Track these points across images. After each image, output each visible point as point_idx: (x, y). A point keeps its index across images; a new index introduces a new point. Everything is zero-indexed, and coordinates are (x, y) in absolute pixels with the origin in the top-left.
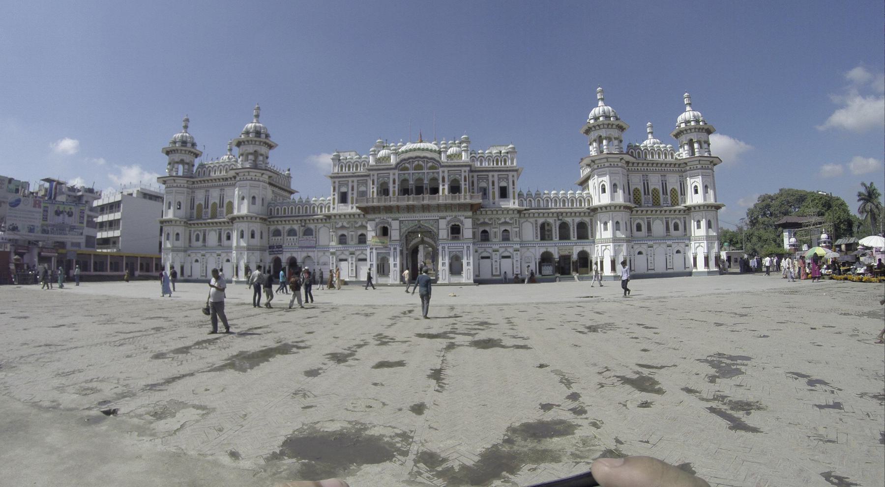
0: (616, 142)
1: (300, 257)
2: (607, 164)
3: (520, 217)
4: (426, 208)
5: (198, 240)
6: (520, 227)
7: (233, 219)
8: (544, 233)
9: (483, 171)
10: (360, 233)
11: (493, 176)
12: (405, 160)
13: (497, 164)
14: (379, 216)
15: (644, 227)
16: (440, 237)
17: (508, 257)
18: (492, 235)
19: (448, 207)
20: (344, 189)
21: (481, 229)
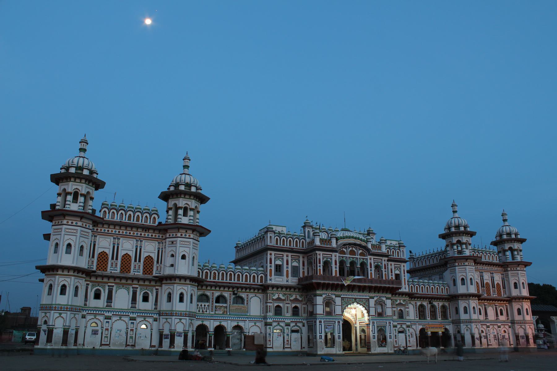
1: (229, 326)
2: (467, 264)
5: (97, 296)
7: (161, 280)
10: (294, 305)
12: (345, 245)
20: (279, 262)
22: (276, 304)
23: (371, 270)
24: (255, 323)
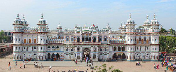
0: (133, 29)
1: (55, 53)
5: (25, 48)
6: (109, 47)
7: (37, 44)
8: (115, 49)
15: (139, 48)
17: (106, 55)
19: (93, 44)
20: (67, 38)
21: (100, 48)
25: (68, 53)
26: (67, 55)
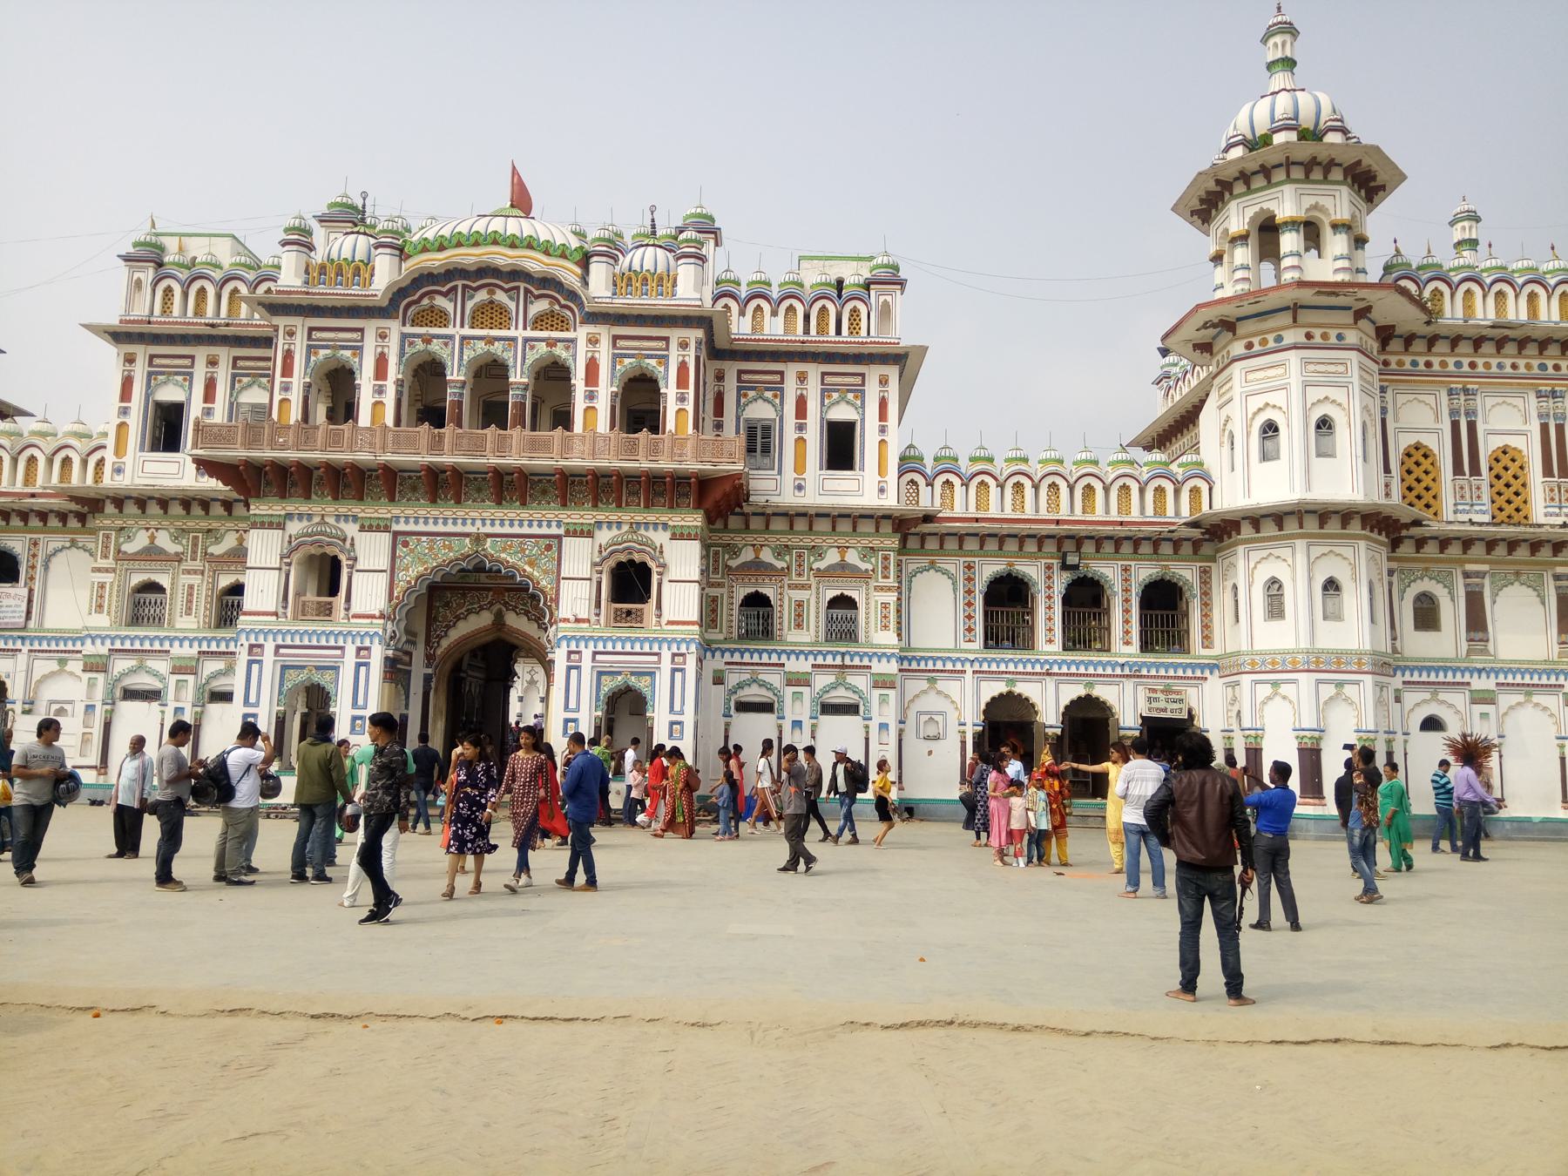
2: (1290, 337)
3: (903, 549)
4: (510, 486)
6: (903, 590)
9: (760, 355)
10: (225, 581)
11: (802, 378)
13: (822, 330)
14: (304, 508)
15: (1452, 613)
16: (564, 611)
17: (851, 709)
18: (784, 614)
20: (170, 393)
21: (742, 592)
22: (137, 579)
23: (591, 396)
24: (62, 662)
25: (162, 666)
26: (131, 694)
